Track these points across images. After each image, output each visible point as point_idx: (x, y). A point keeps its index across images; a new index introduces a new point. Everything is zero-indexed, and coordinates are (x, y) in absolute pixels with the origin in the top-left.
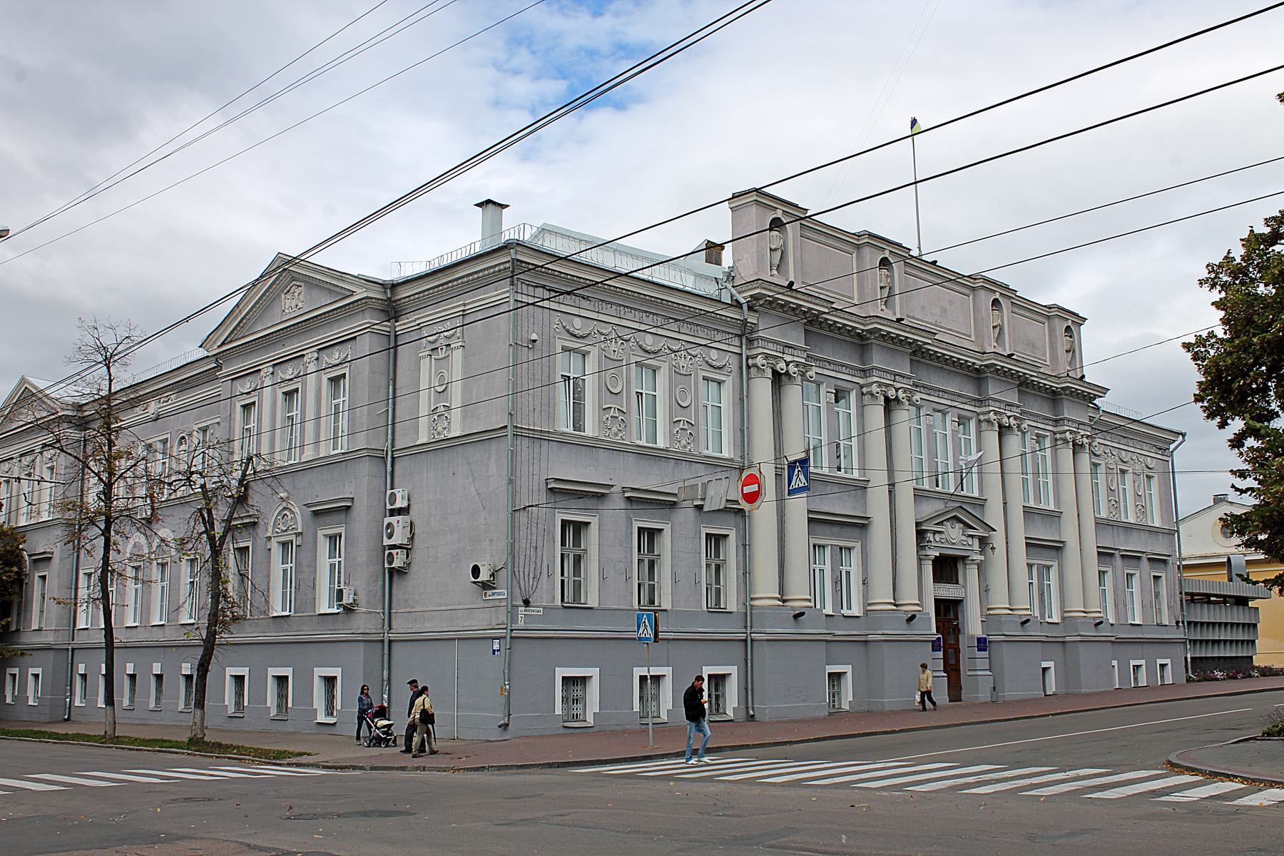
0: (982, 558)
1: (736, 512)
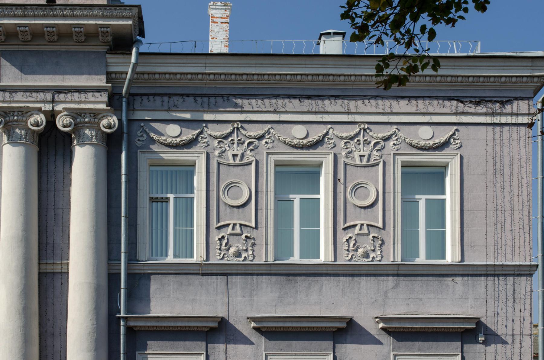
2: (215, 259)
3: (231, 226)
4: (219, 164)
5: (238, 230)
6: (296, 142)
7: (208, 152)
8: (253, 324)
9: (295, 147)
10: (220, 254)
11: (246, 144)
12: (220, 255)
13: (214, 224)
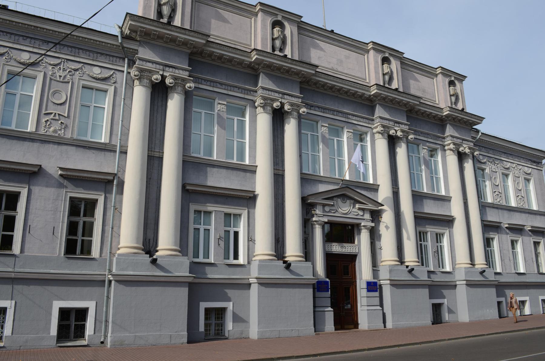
0: (373, 225)
1: (106, 182)
2: (42, 131)
3: (53, 114)
4: (51, 79)
5: (57, 117)
6: (95, 76)
7: (45, 72)
8: (60, 172)
9: (94, 78)
10: (45, 130)
11: (68, 71)
12: (44, 131)
13: (44, 112)
